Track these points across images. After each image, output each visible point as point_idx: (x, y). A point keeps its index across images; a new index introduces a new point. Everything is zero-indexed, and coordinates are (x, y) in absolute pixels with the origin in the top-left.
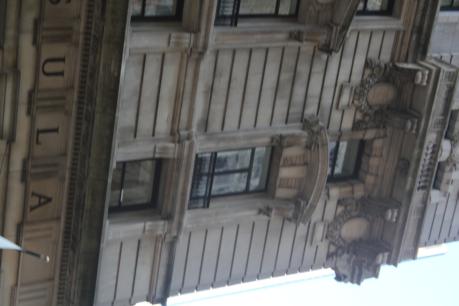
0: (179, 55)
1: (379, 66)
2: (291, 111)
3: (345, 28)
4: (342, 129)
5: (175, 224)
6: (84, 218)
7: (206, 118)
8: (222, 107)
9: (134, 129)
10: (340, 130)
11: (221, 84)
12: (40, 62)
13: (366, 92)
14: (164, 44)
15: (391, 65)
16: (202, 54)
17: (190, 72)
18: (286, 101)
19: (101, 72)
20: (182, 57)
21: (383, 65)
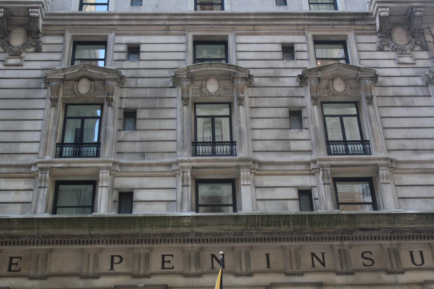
0: (395, 176)
1: (381, 42)
2: (422, 95)
3: (359, 69)
4: (429, 58)
8: (426, 142)
10: (430, 59)
11: (410, 144)
12: (415, 268)
13: (400, 47)
14: (389, 186)
15: (379, 34)
16: (392, 160)
17: (405, 166)
18: (415, 99)
19: (416, 226)
20: (396, 173)
21: (379, 40)
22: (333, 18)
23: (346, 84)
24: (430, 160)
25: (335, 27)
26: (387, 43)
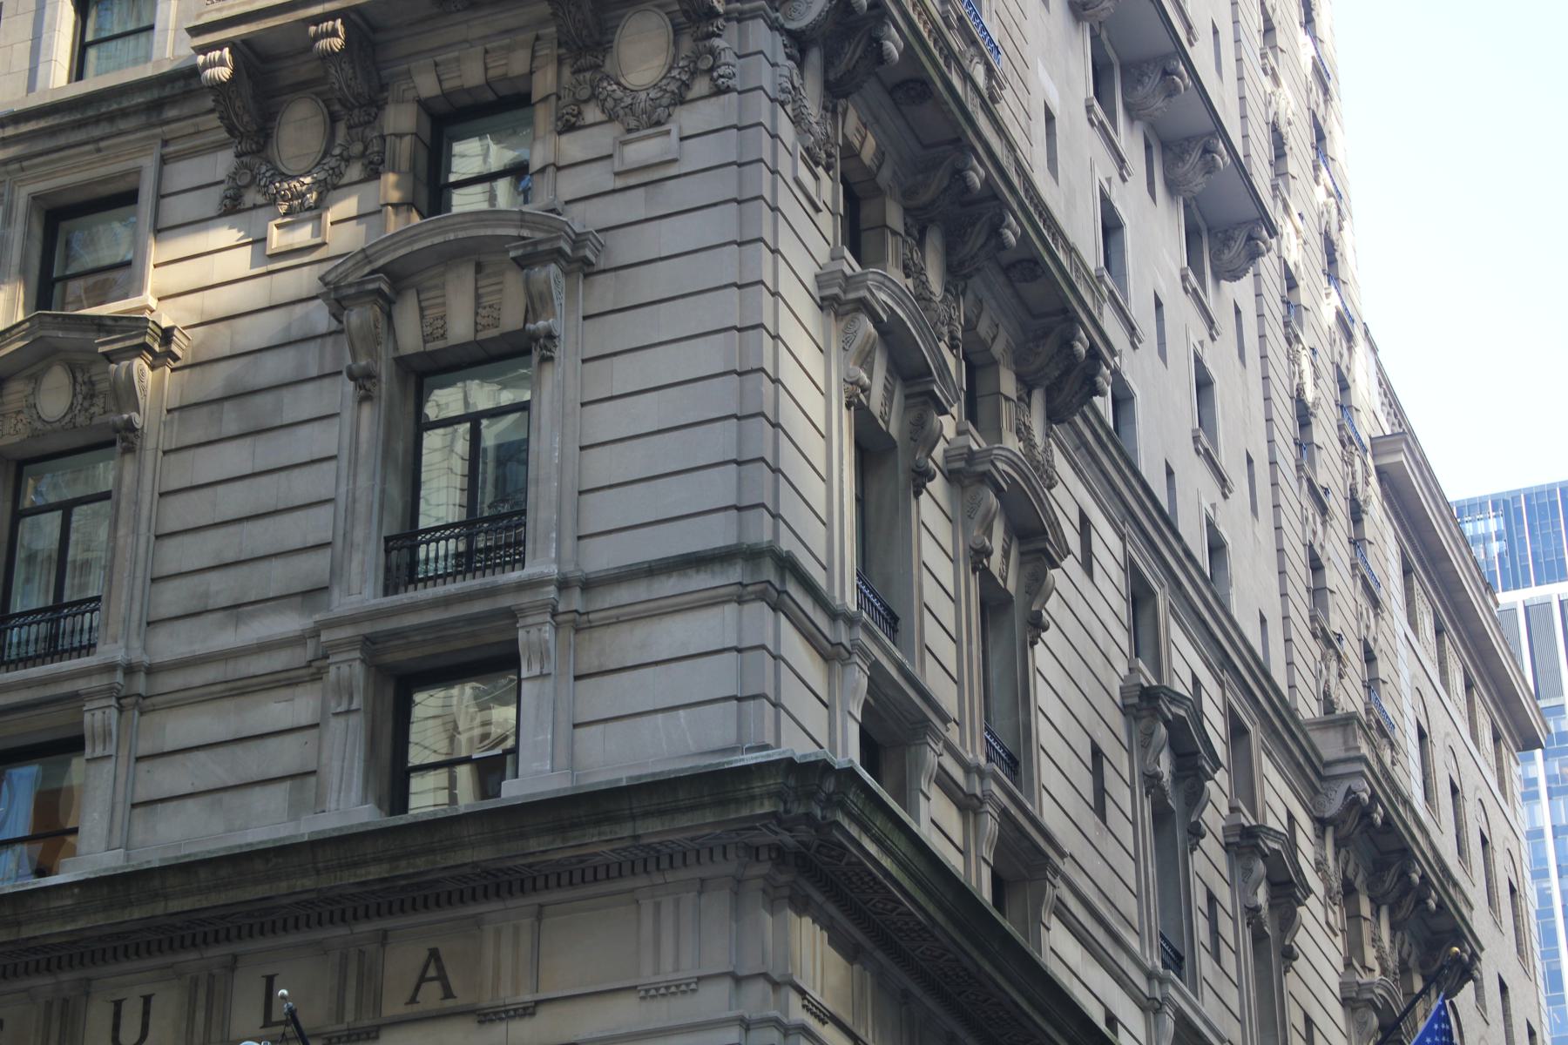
1: (233, 177)
5: (525, 599)
6: (411, 871)
7: (299, 599)
9: (297, 782)
14: (108, 766)
18: (287, 395)
19: (80, 924)
22: (91, 113)
23: (74, 385)
24: (255, 642)
25: (103, 144)
26: (254, 178)
